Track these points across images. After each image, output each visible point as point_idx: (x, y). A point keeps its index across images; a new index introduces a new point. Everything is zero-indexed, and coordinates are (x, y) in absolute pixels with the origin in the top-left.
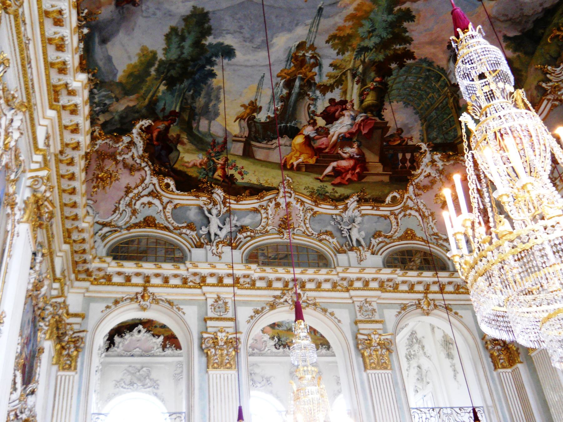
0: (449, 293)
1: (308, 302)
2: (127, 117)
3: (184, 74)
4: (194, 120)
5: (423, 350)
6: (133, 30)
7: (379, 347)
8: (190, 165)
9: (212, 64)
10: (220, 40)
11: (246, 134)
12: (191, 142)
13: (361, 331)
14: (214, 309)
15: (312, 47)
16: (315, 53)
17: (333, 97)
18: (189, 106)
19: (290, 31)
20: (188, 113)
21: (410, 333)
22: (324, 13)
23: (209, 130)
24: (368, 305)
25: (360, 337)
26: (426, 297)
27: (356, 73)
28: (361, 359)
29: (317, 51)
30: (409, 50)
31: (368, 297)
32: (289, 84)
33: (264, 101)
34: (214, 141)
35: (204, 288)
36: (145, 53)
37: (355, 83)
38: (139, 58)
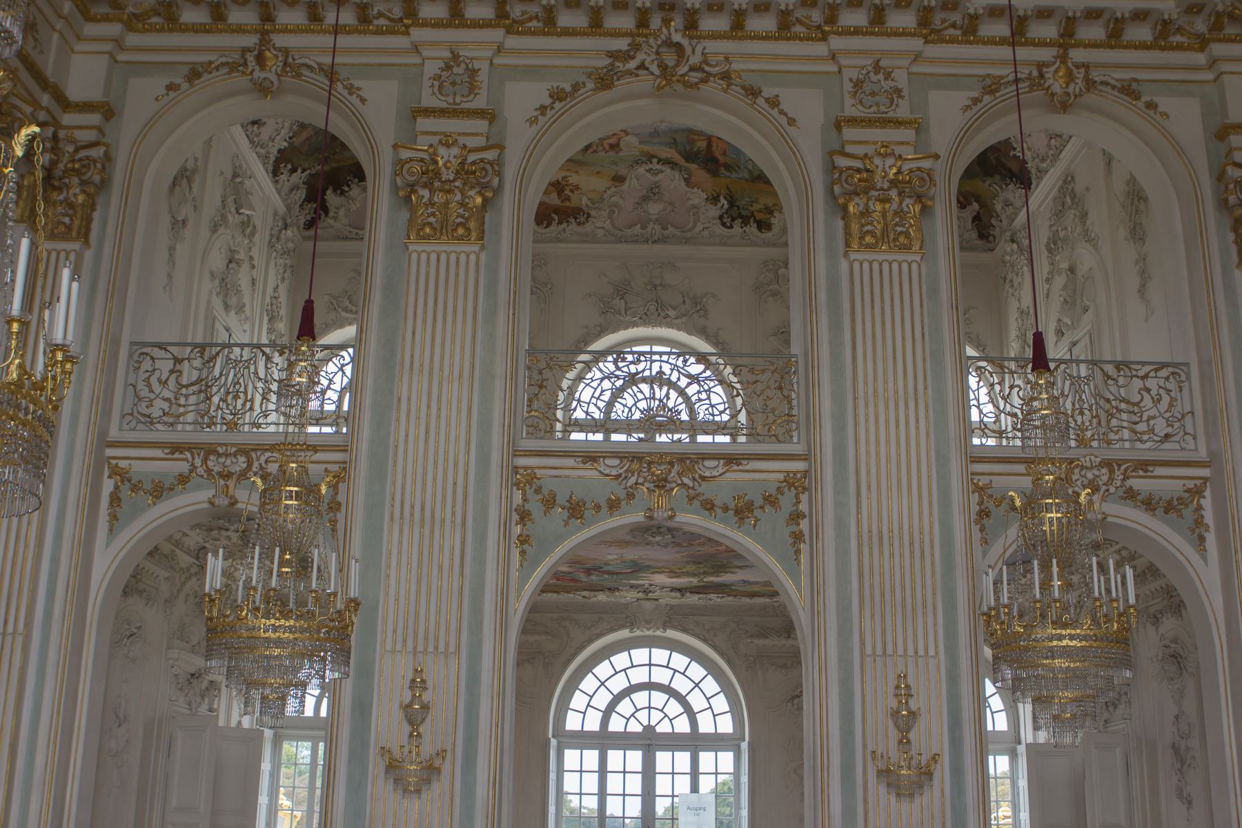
0: (1136, 48)
1: (707, 68)
5: (1084, 223)
7: (893, 193)
13: (849, 149)
14: (441, 87)
21: (1060, 183)
24: (881, 77)
25: (842, 162)
26: (1063, 58)
28: (841, 223)
31: (882, 52)
35: (413, 31)
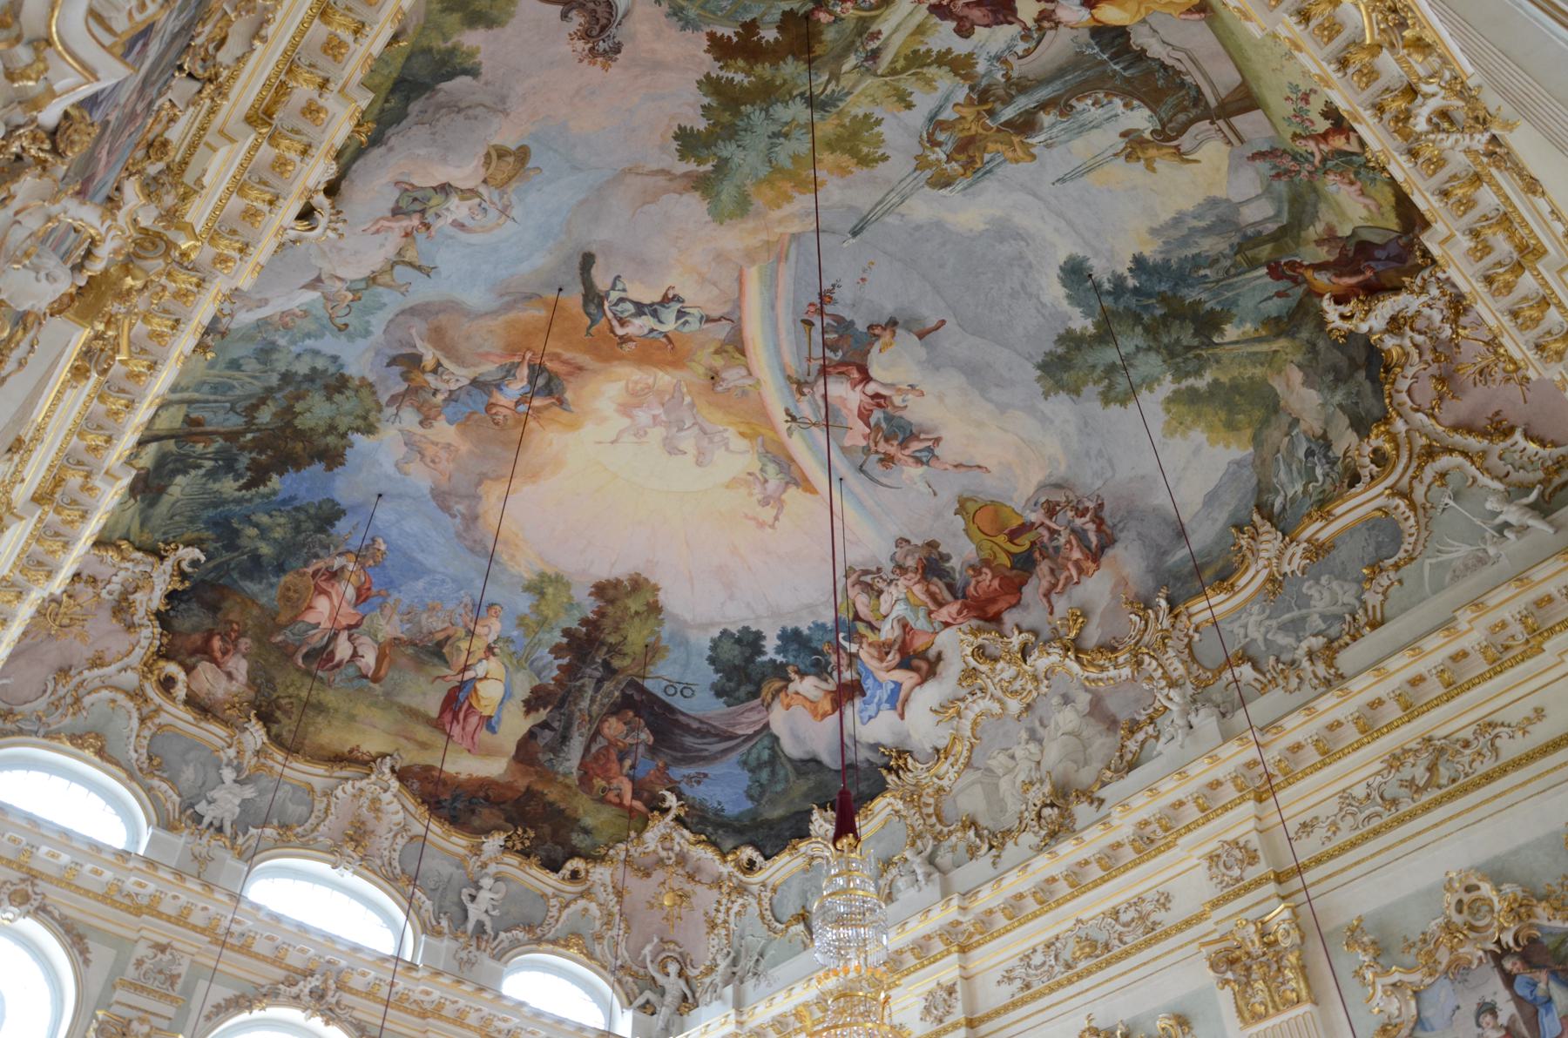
2: (1335, 369)
3: (1178, 312)
4: (1260, 233)
6: (1143, 477)
8: (1368, 201)
9: (1118, 282)
10: (1065, 305)
11: (1205, 124)
12: (1315, 217)
15: (921, 163)
16: (924, 147)
17: (956, 38)
18: (1239, 258)
19: (939, 225)
20: (1256, 251)
22: (853, 222)
23: (1258, 197)
27: (866, 59)
29: (918, 150)
30: (717, 59)
32: (1025, 125)
33: (1108, 139)
34: (1278, 175)
36: (1174, 423)
37: (882, 37)
38: (1189, 428)
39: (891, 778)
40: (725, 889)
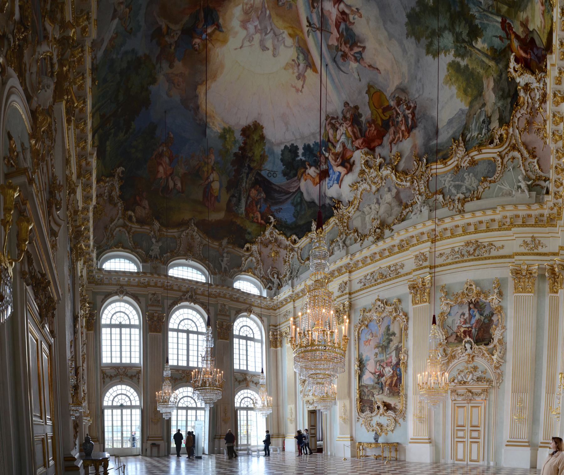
39: (335, 211)
40: (288, 250)
